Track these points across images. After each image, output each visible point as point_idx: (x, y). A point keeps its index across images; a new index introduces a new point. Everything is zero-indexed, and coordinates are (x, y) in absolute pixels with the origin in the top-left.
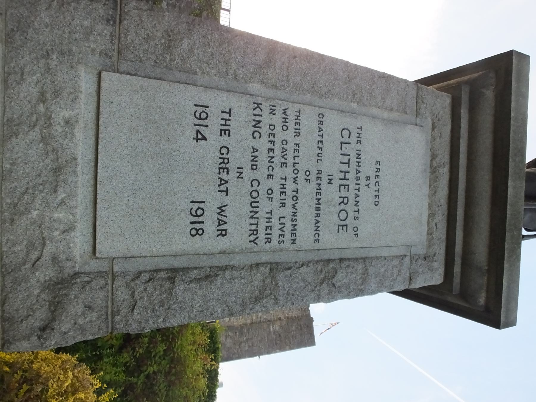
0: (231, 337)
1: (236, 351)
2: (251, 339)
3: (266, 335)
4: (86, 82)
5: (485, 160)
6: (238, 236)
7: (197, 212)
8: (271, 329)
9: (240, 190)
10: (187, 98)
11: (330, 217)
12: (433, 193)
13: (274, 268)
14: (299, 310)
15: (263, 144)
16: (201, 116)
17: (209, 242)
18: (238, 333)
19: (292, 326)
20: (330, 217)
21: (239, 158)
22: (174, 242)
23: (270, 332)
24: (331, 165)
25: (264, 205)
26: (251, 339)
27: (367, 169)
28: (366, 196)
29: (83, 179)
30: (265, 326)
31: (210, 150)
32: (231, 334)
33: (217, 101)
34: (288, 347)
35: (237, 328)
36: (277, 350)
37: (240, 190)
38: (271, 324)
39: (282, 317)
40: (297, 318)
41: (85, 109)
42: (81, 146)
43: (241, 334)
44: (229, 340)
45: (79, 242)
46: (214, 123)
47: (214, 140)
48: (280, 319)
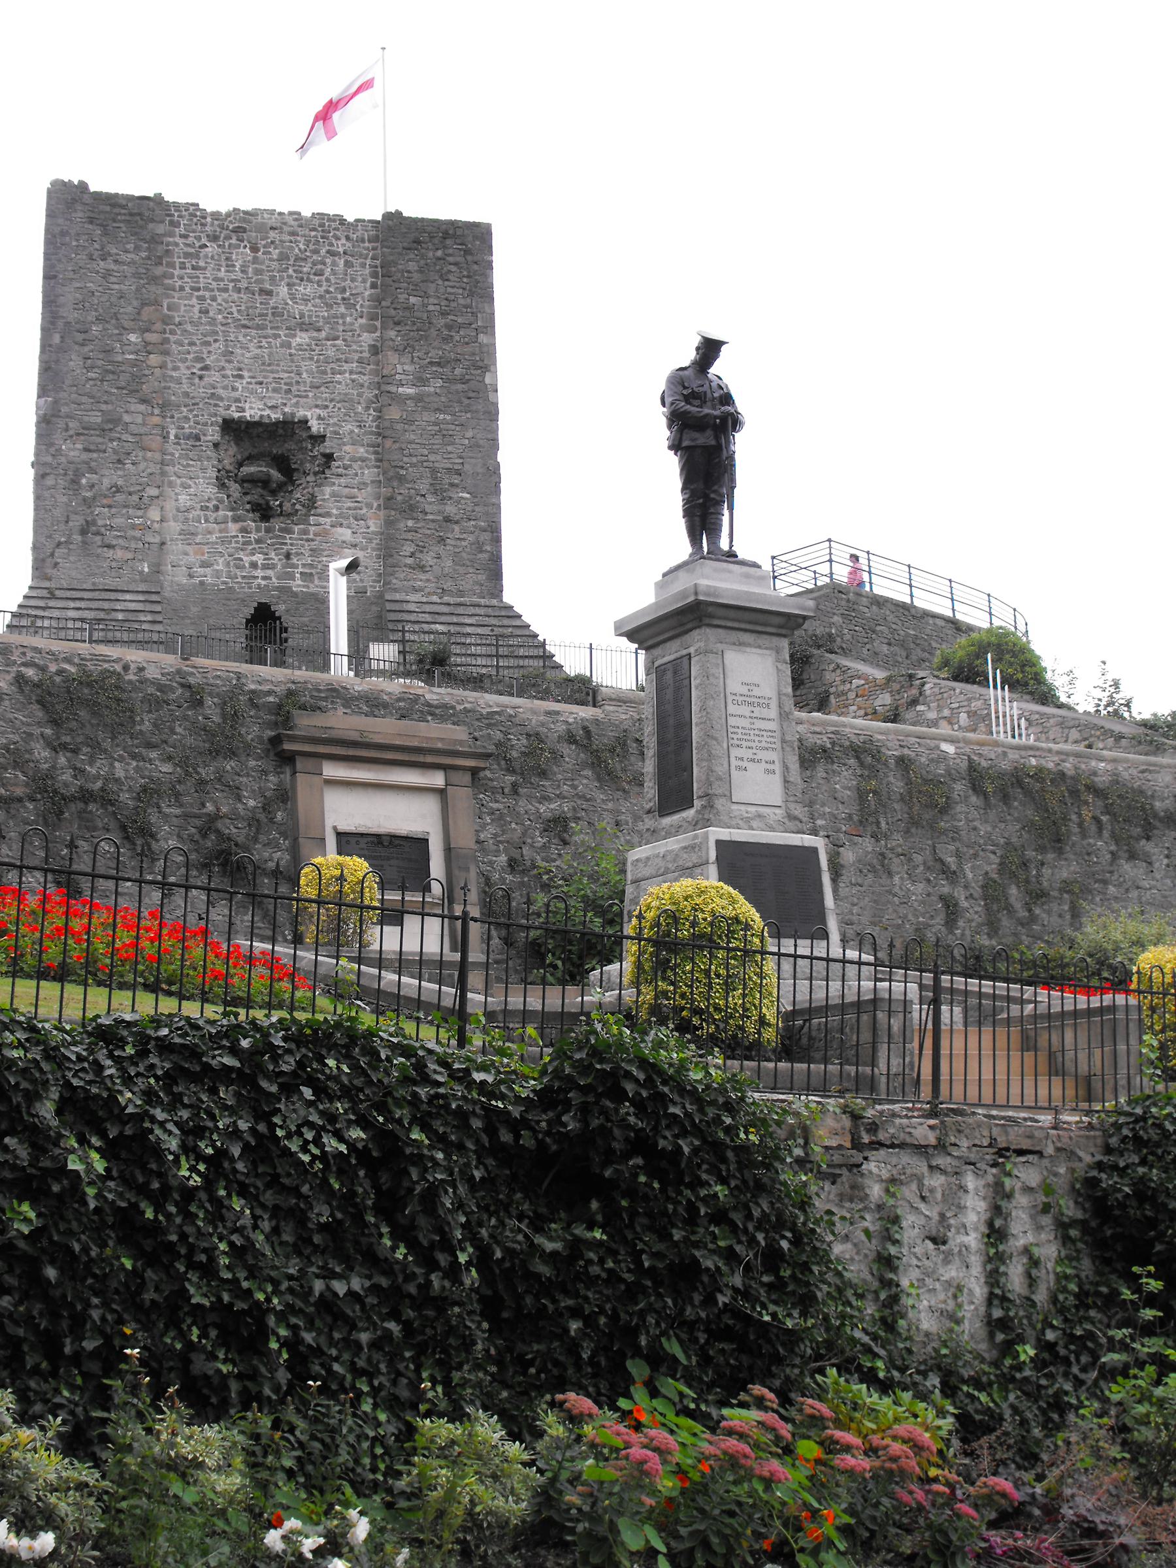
0: (421, 549)
1: (471, 538)
3: (426, 416)
4: (734, 807)
5: (740, 614)
7: (768, 771)
8: (410, 391)
9: (762, 755)
10: (734, 772)
11: (765, 713)
12: (749, 645)
13: (783, 741)
14: (347, 263)
15: (744, 744)
16: (739, 768)
17: (777, 767)
18: (410, 523)
19: (409, 308)
20: (765, 713)
21: (749, 754)
22: (776, 781)
23: (418, 399)
24: (745, 710)
25: (764, 744)
26: (434, 471)
27: (744, 690)
28: (756, 692)
29: (762, 810)
30: (394, 413)
31: (749, 765)
32: (409, 548)
33: (734, 763)
34: (483, 338)
35: (389, 523)
36: (488, 380)
38: (393, 389)
39: (367, 339)
40: (385, 276)
41: (743, 808)
42: (752, 809)
43: (410, 509)
44: (428, 559)
45: (778, 811)
46: (740, 763)
47: (745, 764)
48: (375, 350)
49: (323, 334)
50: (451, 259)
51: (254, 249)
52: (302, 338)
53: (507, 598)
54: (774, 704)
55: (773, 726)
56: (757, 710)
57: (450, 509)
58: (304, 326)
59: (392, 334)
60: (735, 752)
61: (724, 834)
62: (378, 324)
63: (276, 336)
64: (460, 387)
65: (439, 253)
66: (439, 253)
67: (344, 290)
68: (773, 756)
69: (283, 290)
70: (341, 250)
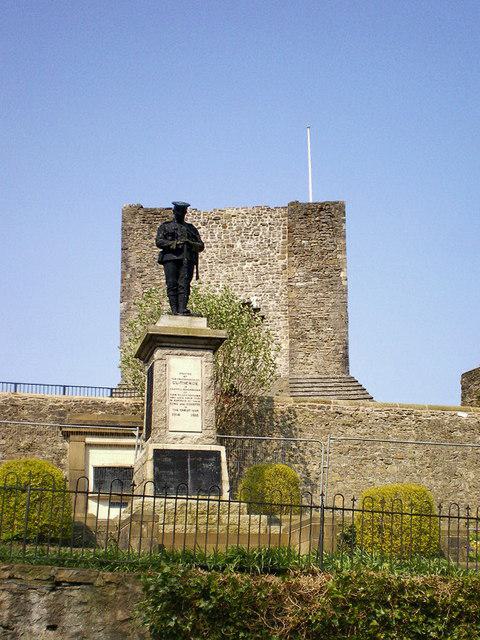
0: (308, 355)
1: (333, 348)
2: (314, 320)
6: (199, 408)
9: (189, 407)
11: (194, 387)
16: (174, 415)
19: (302, 246)
20: (194, 387)
21: (183, 407)
24: (182, 386)
25: (192, 402)
26: (314, 320)
27: (181, 377)
28: (188, 377)
30: (294, 294)
31: (181, 413)
33: (171, 412)
35: (291, 344)
37: (189, 407)
39: (281, 263)
43: (303, 337)
48: (284, 267)
49: (258, 263)
50: (324, 221)
51: (224, 227)
52: (249, 265)
53: (351, 374)
54: (199, 383)
55: (199, 393)
56: (189, 387)
57: (322, 336)
58: (250, 260)
59: (293, 259)
60: (172, 407)
61: (160, 446)
62: (286, 255)
63: (236, 266)
64: (328, 280)
65: (317, 219)
66: (317, 219)
67: (269, 241)
68: (199, 408)
69: (238, 245)
70: (267, 222)
